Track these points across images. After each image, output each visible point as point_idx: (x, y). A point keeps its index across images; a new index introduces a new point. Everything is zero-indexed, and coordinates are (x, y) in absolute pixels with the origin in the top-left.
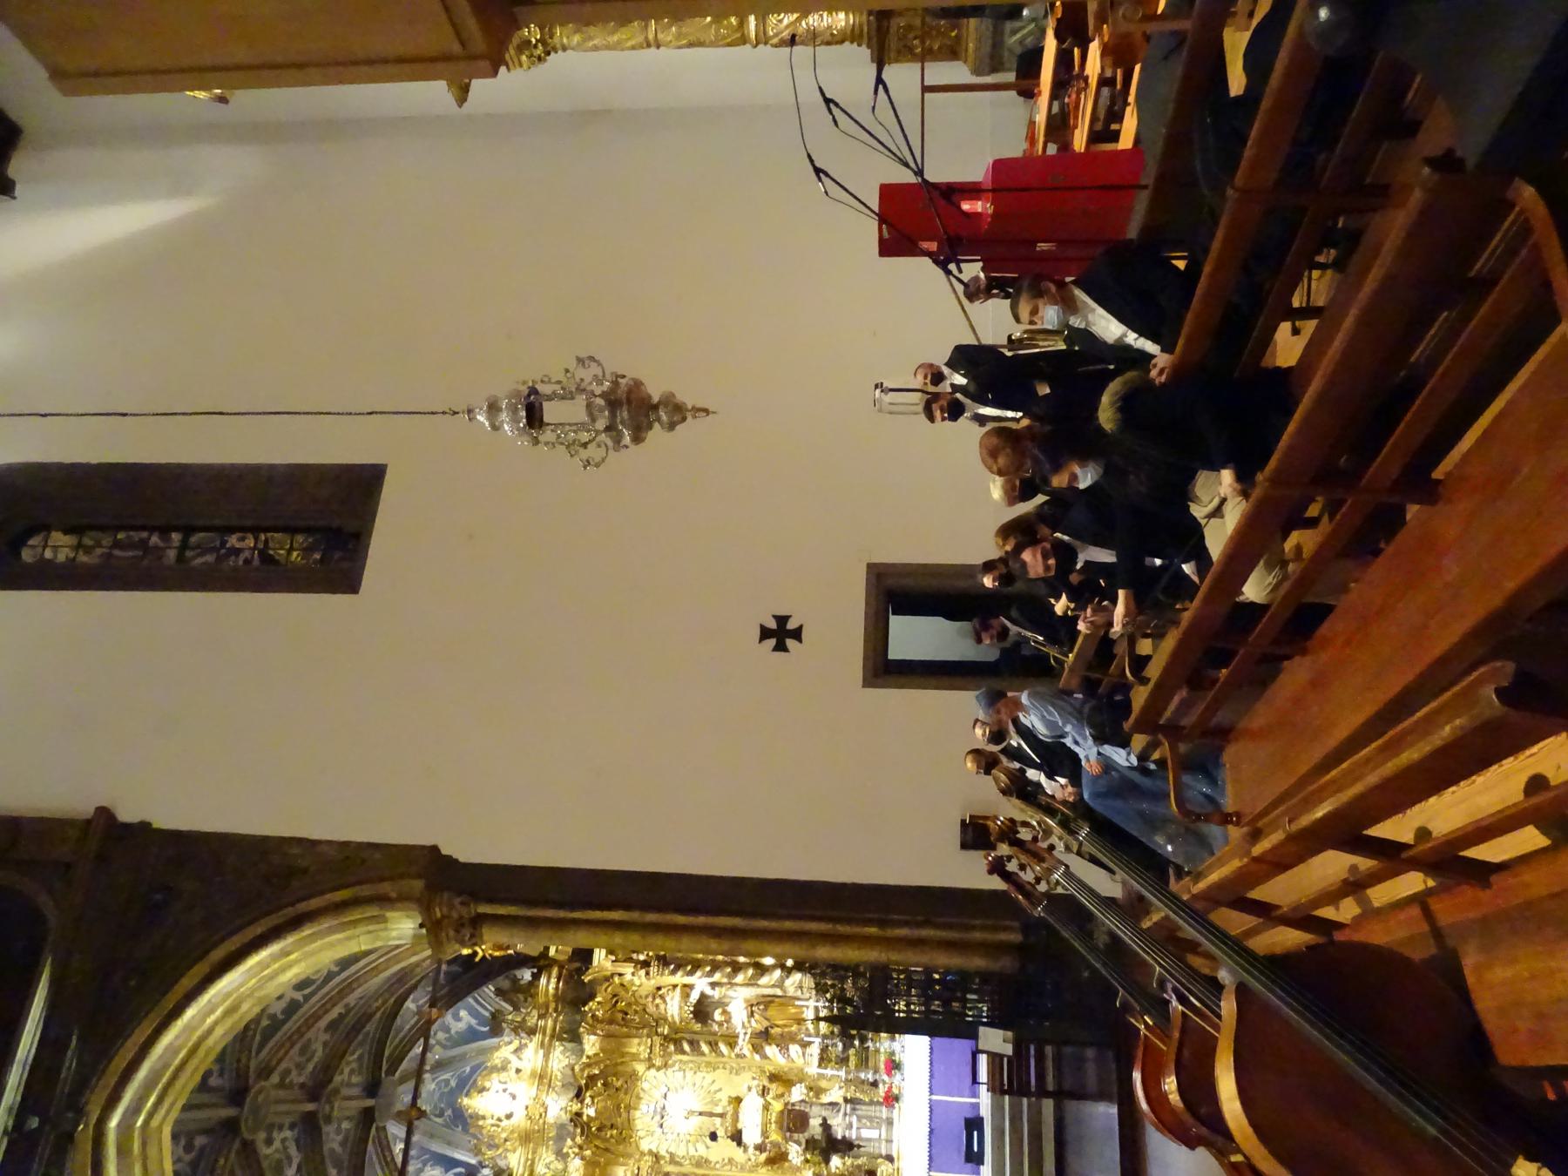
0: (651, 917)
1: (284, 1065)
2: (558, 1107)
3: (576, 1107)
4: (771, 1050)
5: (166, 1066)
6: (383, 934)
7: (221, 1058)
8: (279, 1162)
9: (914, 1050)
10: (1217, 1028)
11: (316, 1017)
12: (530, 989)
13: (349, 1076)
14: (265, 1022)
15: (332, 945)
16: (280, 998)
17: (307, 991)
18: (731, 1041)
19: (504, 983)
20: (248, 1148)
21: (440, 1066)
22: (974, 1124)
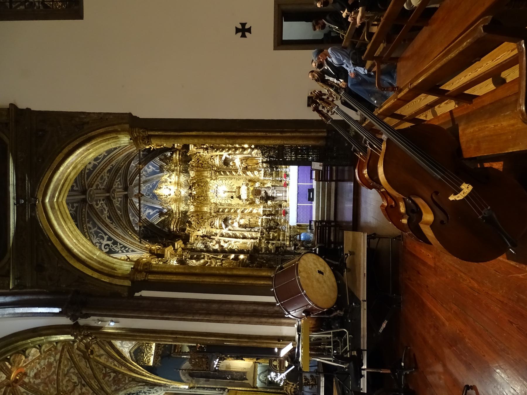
0: (206, 133)
1: (96, 183)
2: (184, 192)
3: (190, 192)
4: (249, 173)
5: (59, 184)
6: (119, 142)
7: (76, 181)
8: (101, 209)
9: (293, 170)
10: (380, 153)
11: (103, 169)
12: (170, 158)
13: (118, 185)
14: (87, 171)
15: (103, 146)
16: (90, 163)
17: (98, 161)
18: (236, 171)
20: (91, 206)
22: (311, 190)
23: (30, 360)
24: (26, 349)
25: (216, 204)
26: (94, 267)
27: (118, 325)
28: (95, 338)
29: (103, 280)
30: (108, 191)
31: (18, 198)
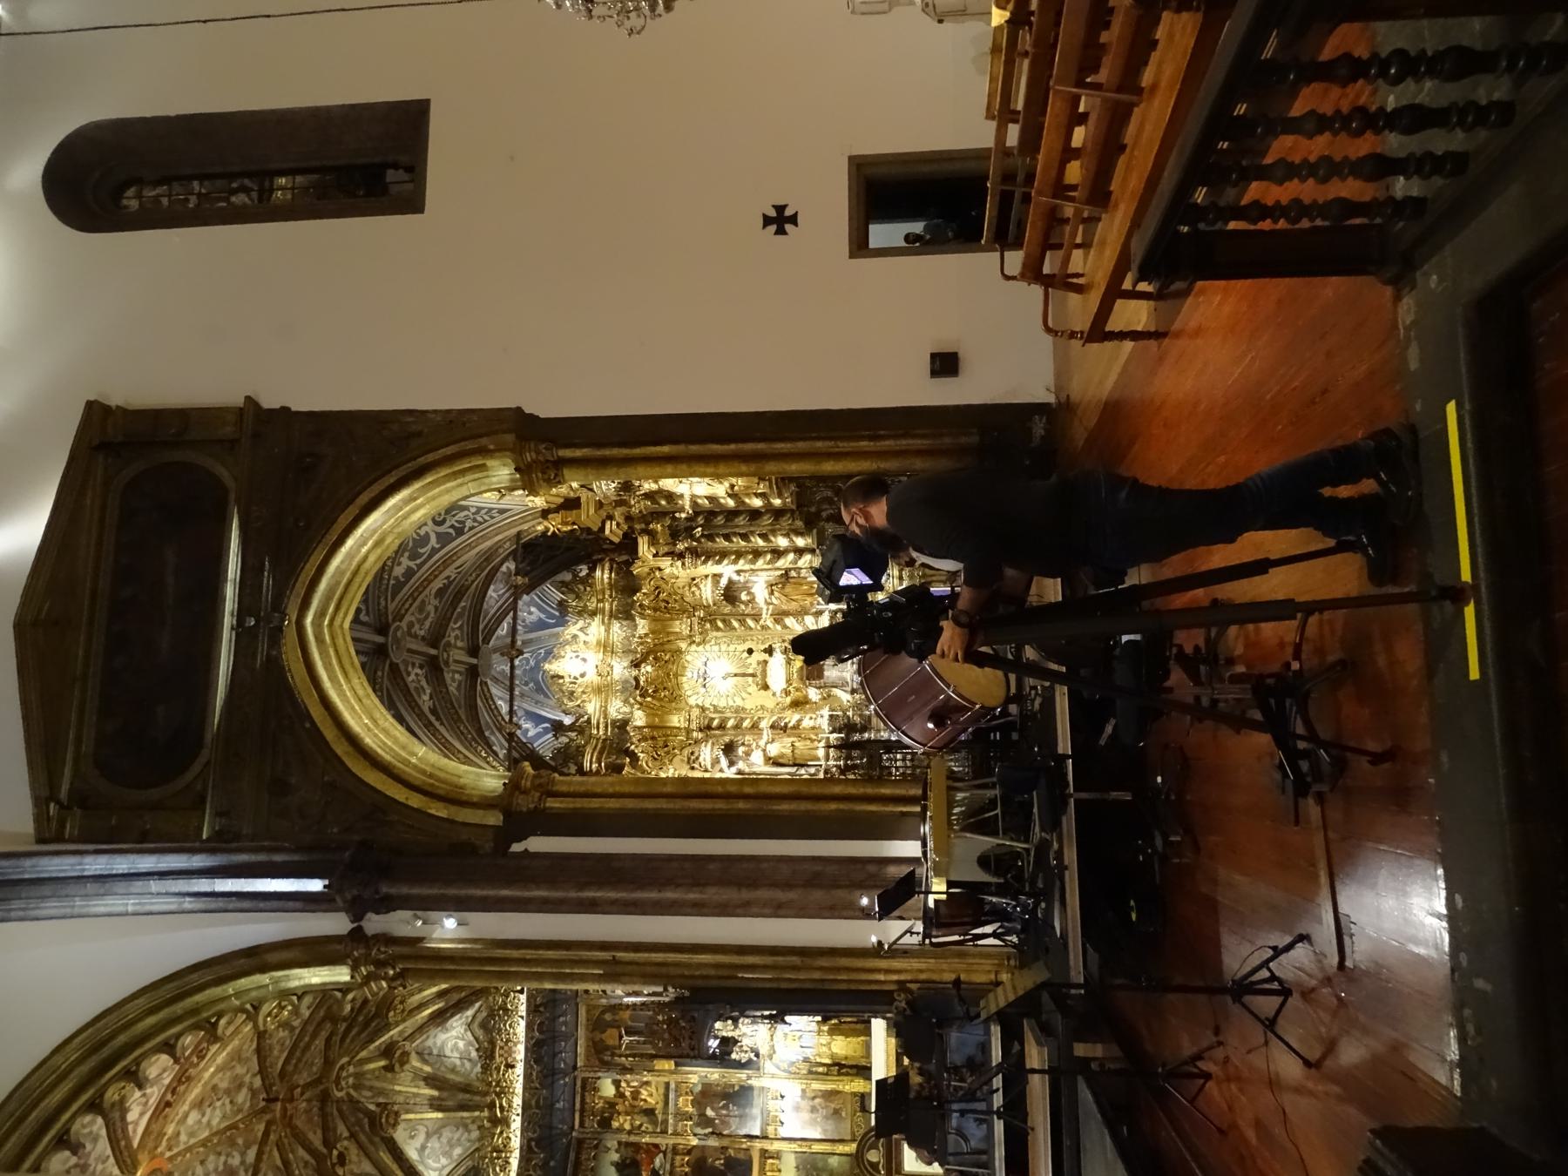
0: (694, 449)
4: (790, 621)
5: (338, 583)
11: (429, 581)
12: (587, 581)
15: (448, 491)
18: (757, 617)
19: (567, 576)
20: (394, 669)
21: (524, 642)
23: (182, 1147)
24: (220, 1015)
25: (703, 709)
26: (412, 780)
27: (464, 933)
28: (402, 975)
29: (432, 812)
30: (435, 646)
31: (241, 614)
